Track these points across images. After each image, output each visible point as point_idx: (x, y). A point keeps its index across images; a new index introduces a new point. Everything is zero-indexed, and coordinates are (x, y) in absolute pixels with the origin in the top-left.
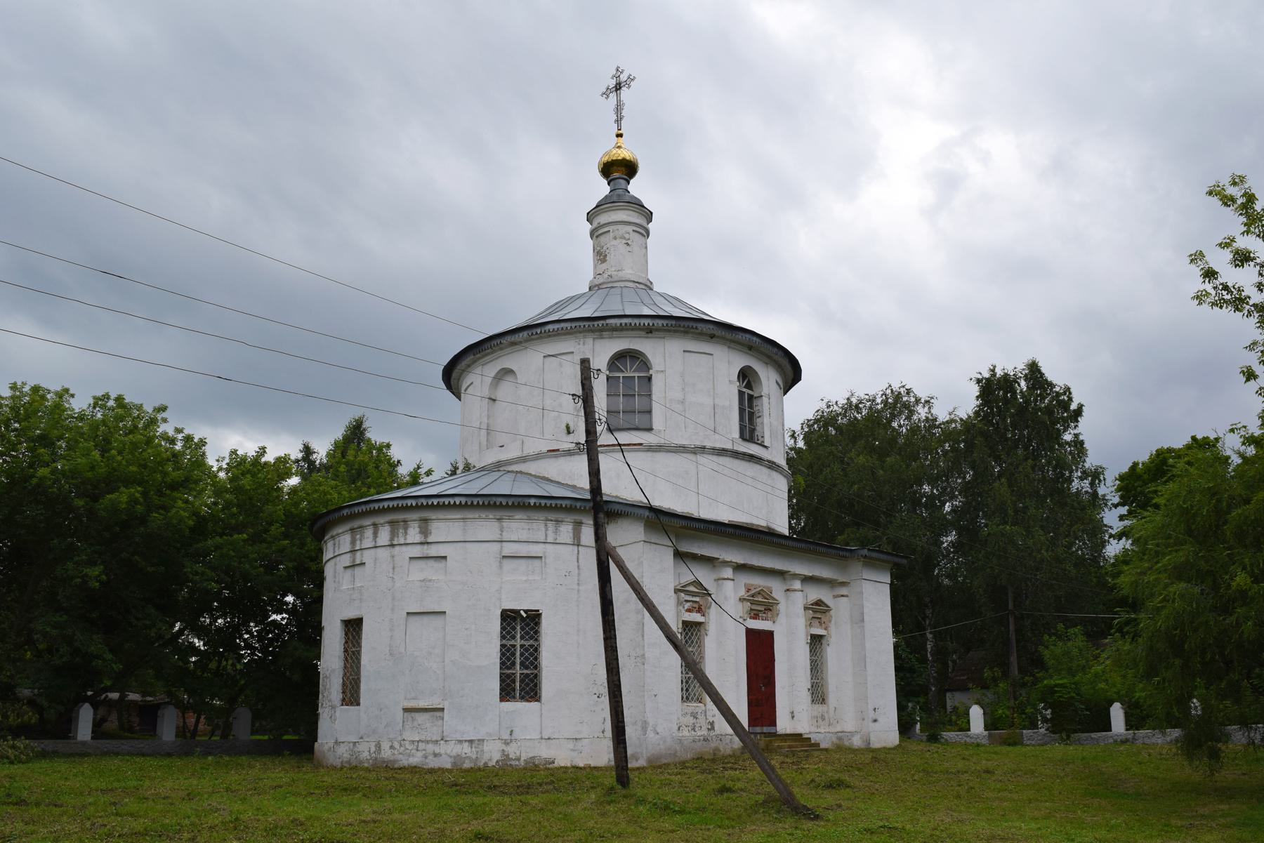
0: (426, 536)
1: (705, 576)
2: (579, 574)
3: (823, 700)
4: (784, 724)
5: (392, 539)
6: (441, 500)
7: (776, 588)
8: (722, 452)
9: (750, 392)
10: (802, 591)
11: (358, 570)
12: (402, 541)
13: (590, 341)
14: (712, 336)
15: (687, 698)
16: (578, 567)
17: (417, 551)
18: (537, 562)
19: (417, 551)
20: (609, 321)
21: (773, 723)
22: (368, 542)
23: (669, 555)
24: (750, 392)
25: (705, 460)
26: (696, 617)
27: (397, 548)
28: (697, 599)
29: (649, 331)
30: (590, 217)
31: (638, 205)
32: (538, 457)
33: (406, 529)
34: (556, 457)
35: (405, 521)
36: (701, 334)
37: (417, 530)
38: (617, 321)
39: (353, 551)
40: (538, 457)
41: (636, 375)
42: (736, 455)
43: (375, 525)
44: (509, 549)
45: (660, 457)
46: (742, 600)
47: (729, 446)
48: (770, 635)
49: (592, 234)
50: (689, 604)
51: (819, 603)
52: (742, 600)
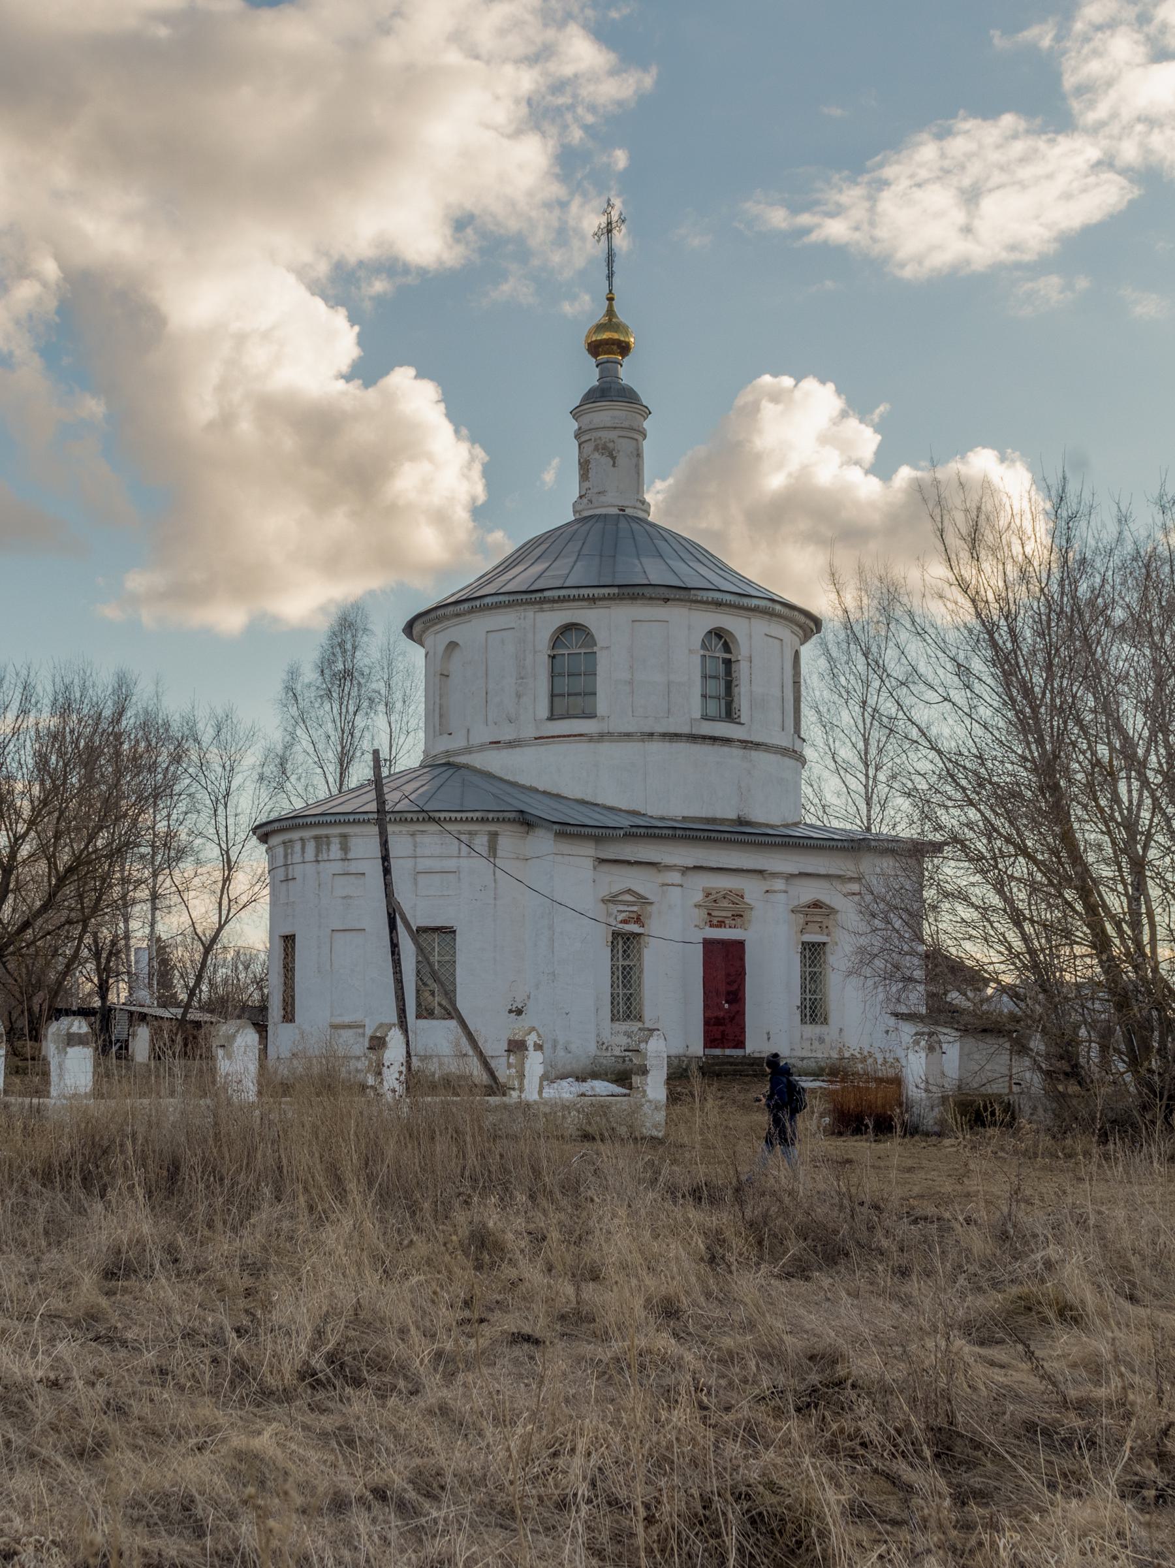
0: (346, 854)
1: (641, 882)
2: (495, 888)
3: (825, 1019)
4: (756, 1045)
5: (317, 856)
6: (357, 817)
7: (751, 889)
8: (674, 737)
9: (727, 656)
10: (786, 892)
11: (291, 883)
12: (325, 858)
13: (530, 614)
14: (666, 600)
15: (628, 1016)
16: (495, 880)
17: (337, 867)
18: (451, 876)
19: (337, 867)
20: (547, 594)
21: (741, 1044)
22: (297, 858)
23: (589, 863)
24: (727, 656)
25: (655, 747)
26: (634, 928)
27: (322, 864)
28: (635, 908)
29: (593, 600)
30: (576, 413)
31: (629, 396)
32: (482, 748)
33: (328, 844)
34: (498, 749)
35: (327, 837)
36: (651, 598)
37: (338, 846)
38: (556, 593)
39: (286, 865)
40: (482, 748)
41: (583, 651)
42: (693, 738)
43: (302, 839)
44: (423, 864)
45: (605, 747)
46: (697, 906)
47: (685, 730)
48: (739, 945)
49: (577, 436)
50: (624, 915)
51: (817, 905)
52: (697, 906)
